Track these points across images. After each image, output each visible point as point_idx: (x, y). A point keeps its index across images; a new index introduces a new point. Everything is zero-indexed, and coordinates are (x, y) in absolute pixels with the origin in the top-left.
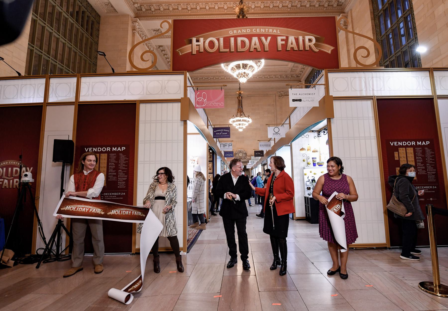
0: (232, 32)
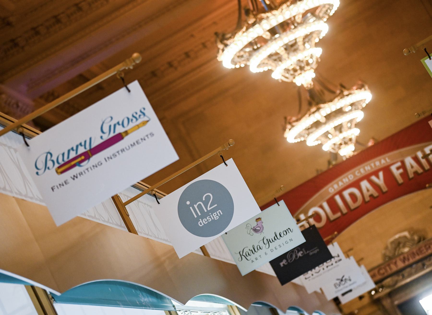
0: (332, 188)
